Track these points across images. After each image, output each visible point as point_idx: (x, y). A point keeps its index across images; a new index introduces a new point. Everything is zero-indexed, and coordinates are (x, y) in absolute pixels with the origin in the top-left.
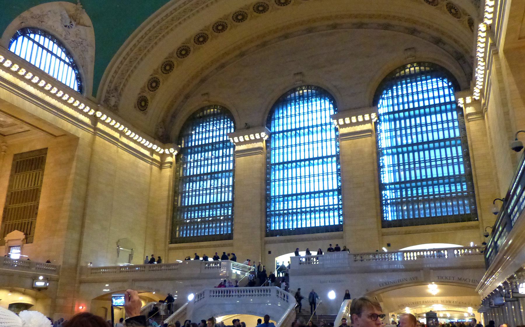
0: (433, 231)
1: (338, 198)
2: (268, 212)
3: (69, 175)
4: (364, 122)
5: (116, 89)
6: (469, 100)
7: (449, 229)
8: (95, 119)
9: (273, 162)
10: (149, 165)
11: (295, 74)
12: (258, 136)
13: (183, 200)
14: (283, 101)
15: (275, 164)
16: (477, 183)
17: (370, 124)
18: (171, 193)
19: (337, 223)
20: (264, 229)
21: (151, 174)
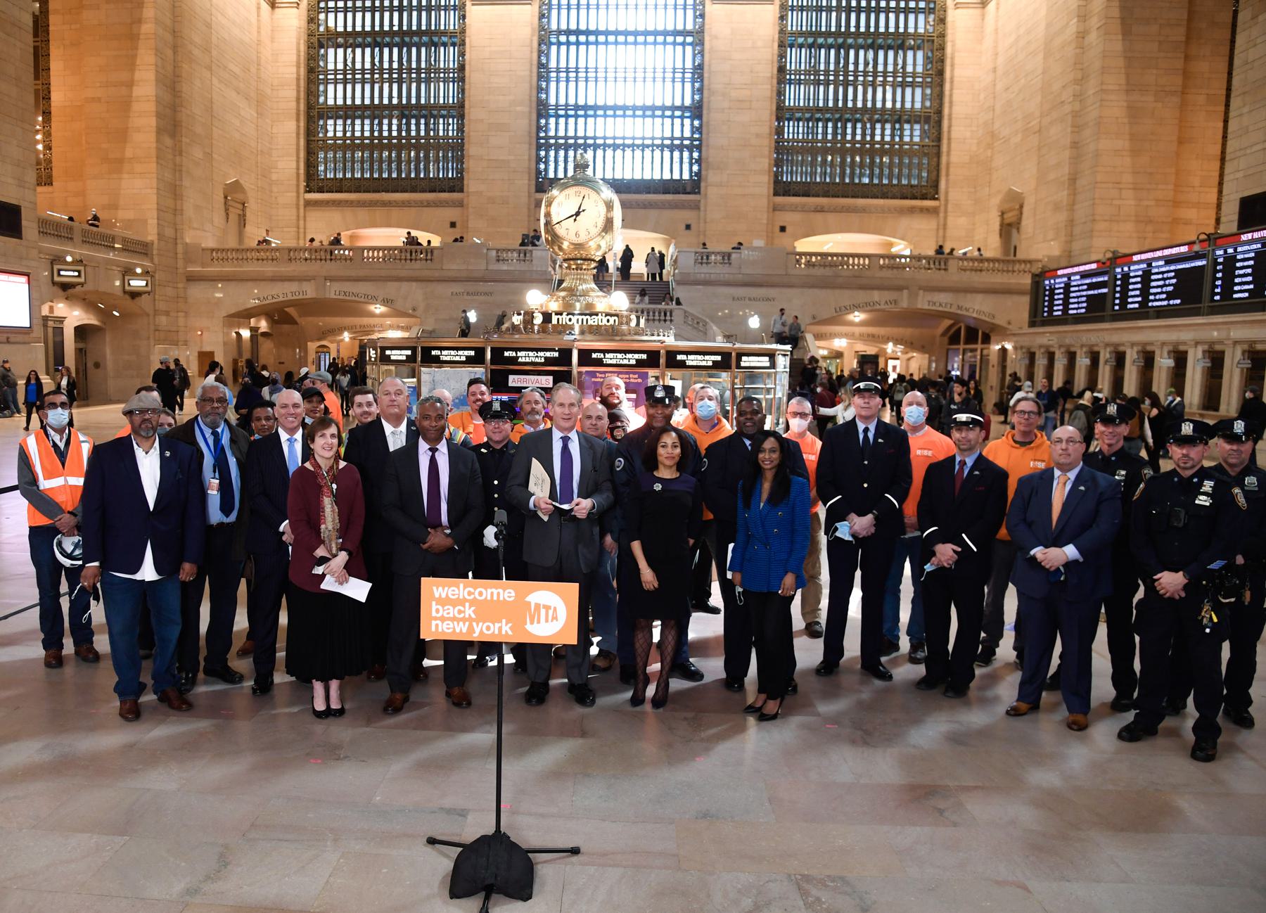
0: (864, 210)
1: (692, 124)
7: (891, 210)
9: (554, 27)
15: (559, 32)
16: (949, 132)
18: (303, 71)
19: (686, 176)
20: (533, 175)
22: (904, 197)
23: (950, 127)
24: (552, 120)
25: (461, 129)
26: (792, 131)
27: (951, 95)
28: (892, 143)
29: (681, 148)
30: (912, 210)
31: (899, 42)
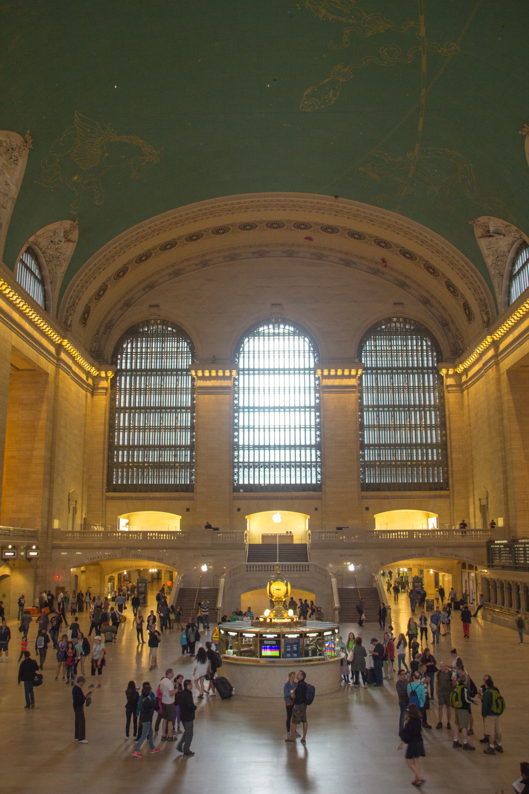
0: (410, 497)
1: (316, 455)
2: (236, 463)
3: (39, 419)
4: (350, 376)
5: (73, 305)
6: (451, 372)
8: (59, 348)
9: (241, 405)
10: (85, 392)
11: (273, 305)
12: (227, 373)
13: (116, 434)
14: (251, 331)
15: (244, 408)
16: (451, 455)
17: (354, 380)
18: (107, 427)
19: (314, 482)
21: (86, 404)
22: (431, 489)
23: (451, 452)
24: (241, 452)
25: (192, 457)
26: (369, 455)
27: (450, 436)
28: (422, 460)
29: (310, 467)
30: (435, 497)
31: (422, 408)
